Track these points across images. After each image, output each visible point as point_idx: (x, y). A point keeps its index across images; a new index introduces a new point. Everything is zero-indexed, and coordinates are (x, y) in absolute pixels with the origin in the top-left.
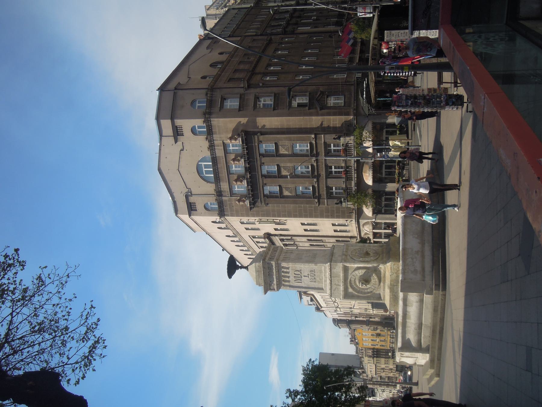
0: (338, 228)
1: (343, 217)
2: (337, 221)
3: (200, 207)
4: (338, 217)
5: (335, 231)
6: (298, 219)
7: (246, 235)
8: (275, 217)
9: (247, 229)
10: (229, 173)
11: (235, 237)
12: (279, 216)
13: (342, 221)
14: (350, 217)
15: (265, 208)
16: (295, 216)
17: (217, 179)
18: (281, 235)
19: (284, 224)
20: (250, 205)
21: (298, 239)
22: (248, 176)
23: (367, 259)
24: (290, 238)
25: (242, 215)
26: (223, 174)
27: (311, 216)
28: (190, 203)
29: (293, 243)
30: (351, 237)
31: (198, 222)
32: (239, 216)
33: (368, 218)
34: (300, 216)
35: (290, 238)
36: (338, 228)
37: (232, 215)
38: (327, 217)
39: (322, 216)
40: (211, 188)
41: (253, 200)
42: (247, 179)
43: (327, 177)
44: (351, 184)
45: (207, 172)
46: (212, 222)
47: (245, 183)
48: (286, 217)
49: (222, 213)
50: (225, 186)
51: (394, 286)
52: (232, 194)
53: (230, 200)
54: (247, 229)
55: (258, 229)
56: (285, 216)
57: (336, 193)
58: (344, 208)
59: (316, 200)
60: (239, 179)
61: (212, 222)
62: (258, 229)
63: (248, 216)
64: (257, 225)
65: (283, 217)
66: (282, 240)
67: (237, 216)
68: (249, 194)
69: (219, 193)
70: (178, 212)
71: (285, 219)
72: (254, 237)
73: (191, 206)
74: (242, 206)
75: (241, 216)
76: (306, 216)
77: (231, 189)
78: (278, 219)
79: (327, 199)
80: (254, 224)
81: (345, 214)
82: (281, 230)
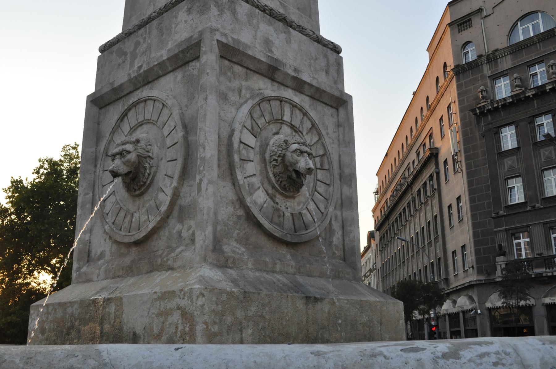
0: (459, 257)
1: (478, 261)
2: (470, 251)
3: (466, 35)
4: (477, 252)
5: (454, 253)
6: (466, 189)
7: (433, 123)
8: (465, 152)
9: (441, 119)
10: (531, 64)
11: (429, 107)
12: (467, 158)
13: (471, 258)
14: (480, 272)
15: (477, 134)
16: (470, 183)
17: (517, 49)
18: (438, 173)
19: (455, 172)
20: (479, 108)
21: (436, 201)
22: (529, 94)
23: (250, 171)
24: (436, 186)
25: (461, 102)
26: (526, 57)
27: (472, 208)
28: (470, 20)
29: (429, 194)
30: (447, 280)
31: (443, 43)
32: (459, 98)
33: (482, 303)
34: (471, 192)
35: (436, 186)
36: (459, 257)
37: (459, 87)
38: (475, 235)
39: (475, 226)
40: (500, 42)
41: (489, 110)
42: (524, 93)
43: (544, 224)
44: (538, 267)
45: (526, 31)
46: (445, 63)
47: (518, 91)
48: (467, 168)
49: (460, 70)
50: (506, 63)
51: (101, 323)
52: (495, 77)
53: (483, 77)
54: (441, 119)
55: (442, 137)
56: (468, 167)
57: (519, 245)
58: (494, 260)
59: (501, 213)
60: (523, 83)
61: (445, 63)
62: (442, 137)
63: (461, 110)
64: (448, 133)
65: (466, 164)
66: (431, 177)
67: (459, 95)
68: (497, 102)
69: (492, 58)
70: (453, 7)
71: (464, 169)
72: (431, 136)
73: (466, 22)
74: (477, 97)
75: (459, 101)
76: (472, 200)
77: (503, 74)
78: (462, 158)
79: (507, 230)
80: (450, 126)
81: (484, 264)
82: (446, 171)
